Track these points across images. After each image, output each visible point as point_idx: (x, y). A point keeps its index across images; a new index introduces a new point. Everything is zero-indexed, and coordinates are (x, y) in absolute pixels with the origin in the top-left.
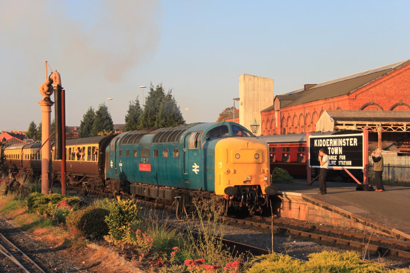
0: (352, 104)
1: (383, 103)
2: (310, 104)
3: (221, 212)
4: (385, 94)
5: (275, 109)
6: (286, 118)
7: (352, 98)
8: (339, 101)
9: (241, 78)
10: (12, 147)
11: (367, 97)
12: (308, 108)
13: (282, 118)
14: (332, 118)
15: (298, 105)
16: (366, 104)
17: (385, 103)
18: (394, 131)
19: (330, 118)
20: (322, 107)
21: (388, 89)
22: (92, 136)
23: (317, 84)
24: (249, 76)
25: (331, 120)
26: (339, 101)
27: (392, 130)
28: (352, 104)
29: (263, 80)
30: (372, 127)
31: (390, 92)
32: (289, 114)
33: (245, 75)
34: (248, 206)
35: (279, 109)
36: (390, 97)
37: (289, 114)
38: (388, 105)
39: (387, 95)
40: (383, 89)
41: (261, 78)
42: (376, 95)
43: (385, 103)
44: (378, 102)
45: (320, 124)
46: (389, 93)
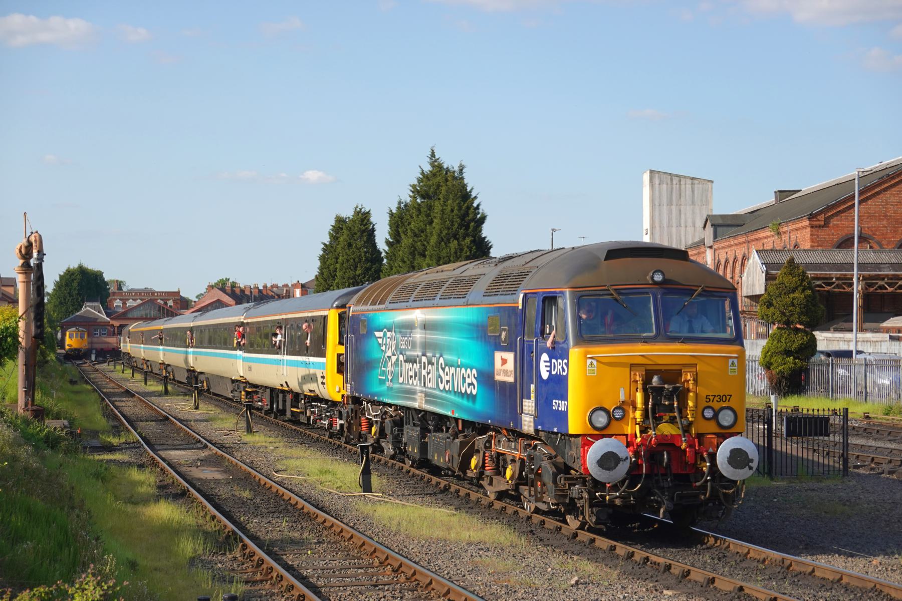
0: (818, 237)
1: (883, 234)
2: (756, 236)
3: (157, 386)
4: (886, 216)
5: (707, 244)
6: (723, 263)
7: (817, 223)
8: (796, 230)
9: (646, 177)
10: (170, 324)
11: (848, 222)
12: (753, 243)
13: (716, 261)
14: (764, 266)
15: (739, 237)
16: (847, 235)
17: (887, 233)
18: (890, 289)
19: (761, 265)
20: (774, 242)
21: (891, 205)
22: (231, 306)
23: (800, 191)
24: (662, 175)
25: (761, 268)
26: (796, 230)
27: (886, 289)
28: (818, 237)
29: (690, 183)
30: (844, 284)
31: (897, 210)
32: (727, 253)
33: (651, 172)
34: (510, 423)
35: (711, 244)
36: (896, 222)
37: (727, 253)
38: (893, 237)
39: (890, 216)
40: (881, 205)
41: (685, 177)
42: (867, 218)
43: (887, 233)
44: (872, 231)
45: (748, 277)
46: (894, 213)
